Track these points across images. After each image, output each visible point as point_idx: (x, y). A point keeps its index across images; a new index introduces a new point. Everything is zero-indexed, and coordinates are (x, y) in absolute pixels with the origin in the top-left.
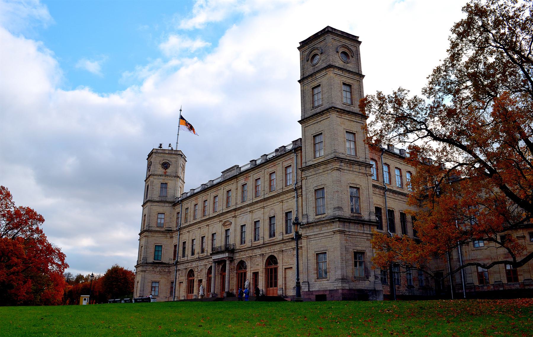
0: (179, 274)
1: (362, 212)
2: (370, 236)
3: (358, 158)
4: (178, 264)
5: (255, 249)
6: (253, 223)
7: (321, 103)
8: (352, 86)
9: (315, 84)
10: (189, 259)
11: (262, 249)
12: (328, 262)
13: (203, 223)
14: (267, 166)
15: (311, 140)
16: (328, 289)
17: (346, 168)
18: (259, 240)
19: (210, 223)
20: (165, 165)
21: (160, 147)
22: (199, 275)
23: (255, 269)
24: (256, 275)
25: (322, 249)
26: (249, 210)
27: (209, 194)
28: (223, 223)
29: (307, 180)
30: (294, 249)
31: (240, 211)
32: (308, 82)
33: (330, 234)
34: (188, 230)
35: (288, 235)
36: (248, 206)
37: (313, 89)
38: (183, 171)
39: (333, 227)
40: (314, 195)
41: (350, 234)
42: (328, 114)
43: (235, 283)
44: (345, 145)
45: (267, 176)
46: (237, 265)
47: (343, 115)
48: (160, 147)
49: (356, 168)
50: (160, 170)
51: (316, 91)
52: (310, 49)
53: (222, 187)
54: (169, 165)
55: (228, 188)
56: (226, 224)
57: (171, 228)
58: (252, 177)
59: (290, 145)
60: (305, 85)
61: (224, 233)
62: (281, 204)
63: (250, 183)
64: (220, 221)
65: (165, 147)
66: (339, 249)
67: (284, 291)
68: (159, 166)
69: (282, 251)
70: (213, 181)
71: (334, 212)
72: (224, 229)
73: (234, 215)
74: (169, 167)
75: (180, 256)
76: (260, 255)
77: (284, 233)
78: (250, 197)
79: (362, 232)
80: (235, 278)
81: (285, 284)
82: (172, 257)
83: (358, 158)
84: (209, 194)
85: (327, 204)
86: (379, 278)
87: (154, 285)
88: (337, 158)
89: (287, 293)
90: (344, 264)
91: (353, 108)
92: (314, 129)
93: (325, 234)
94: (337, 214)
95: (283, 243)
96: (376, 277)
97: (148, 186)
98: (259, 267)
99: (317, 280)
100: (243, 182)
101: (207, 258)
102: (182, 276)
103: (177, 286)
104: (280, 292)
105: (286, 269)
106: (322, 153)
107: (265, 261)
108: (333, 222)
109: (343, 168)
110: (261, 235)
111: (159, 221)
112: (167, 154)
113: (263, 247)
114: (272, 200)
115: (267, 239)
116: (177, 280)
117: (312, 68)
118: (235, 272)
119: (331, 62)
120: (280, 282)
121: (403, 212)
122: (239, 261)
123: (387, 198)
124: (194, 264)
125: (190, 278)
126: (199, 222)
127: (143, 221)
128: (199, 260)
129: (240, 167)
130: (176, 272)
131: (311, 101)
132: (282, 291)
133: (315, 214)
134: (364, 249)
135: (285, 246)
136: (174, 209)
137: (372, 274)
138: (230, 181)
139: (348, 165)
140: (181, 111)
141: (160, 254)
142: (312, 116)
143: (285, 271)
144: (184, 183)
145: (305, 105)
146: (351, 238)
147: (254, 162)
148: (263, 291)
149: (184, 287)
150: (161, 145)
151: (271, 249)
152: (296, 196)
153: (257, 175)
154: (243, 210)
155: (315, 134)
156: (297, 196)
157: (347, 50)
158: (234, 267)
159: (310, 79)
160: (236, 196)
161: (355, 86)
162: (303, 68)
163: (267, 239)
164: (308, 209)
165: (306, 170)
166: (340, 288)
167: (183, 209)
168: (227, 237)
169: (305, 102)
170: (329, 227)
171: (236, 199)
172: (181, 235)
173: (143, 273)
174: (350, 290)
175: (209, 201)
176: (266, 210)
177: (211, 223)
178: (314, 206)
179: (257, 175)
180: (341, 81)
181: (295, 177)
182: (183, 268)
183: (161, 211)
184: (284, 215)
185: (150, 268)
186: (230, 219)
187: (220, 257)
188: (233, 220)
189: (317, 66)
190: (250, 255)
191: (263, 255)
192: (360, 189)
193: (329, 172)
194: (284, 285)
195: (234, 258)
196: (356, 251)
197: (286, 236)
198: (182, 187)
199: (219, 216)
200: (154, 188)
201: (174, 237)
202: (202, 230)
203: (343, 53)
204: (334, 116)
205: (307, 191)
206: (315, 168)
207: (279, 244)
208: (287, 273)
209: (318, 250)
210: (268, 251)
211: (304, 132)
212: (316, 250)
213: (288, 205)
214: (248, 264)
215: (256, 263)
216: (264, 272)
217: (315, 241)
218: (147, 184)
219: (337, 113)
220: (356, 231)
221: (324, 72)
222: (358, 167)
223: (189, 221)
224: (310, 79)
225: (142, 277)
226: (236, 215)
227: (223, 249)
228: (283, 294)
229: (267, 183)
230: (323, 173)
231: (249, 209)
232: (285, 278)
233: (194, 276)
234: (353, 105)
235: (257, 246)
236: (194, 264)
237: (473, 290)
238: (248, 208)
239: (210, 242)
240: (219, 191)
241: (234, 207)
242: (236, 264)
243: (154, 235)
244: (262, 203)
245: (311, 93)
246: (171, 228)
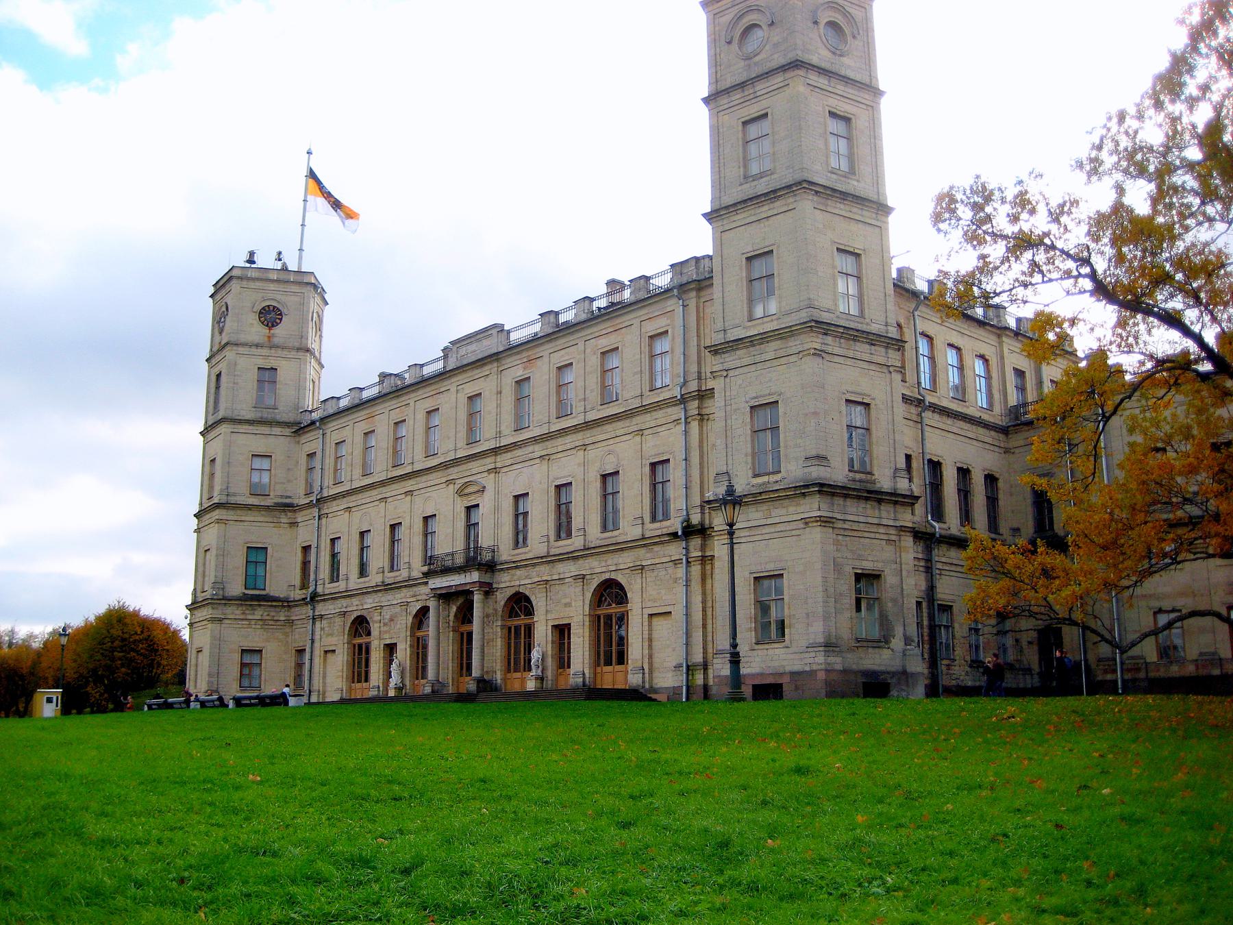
0: (322, 629)
1: (875, 468)
2: (894, 532)
3: (867, 324)
4: (318, 601)
5: (559, 560)
6: (553, 489)
7: (767, 165)
8: (854, 121)
9: (753, 110)
10: (352, 586)
11: (581, 561)
12: (786, 600)
13: (395, 486)
14: (595, 329)
15: (741, 269)
16: (788, 669)
17: (837, 350)
18: (569, 535)
19: (415, 487)
20: (270, 316)
21: (251, 261)
22: (386, 632)
23: (560, 617)
24: (562, 631)
25: (771, 566)
27: (412, 404)
28: (457, 487)
29: (728, 380)
30: (676, 562)
31: (509, 455)
32: (732, 104)
33: (793, 526)
35: (657, 525)
36: (535, 440)
37: (745, 123)
38: (319, 333)
39: (800, 509)
40: (749, 420)
41: (846, 526)
42: (791, 200)
43: (499, 654)
44: (835, 285)
45: (594, 360)
46: (505, 605)
47: (829, 202)
48: (251, 261)
49: (862, 349)
50: (256, 331)
51: (754, 130)
52: (736, 7)
53: (452, 384)
54: (281, 314)
55: (471, 389)
56: (466, 491)
57: (290, 497)
58: (546, 359)
59: (663, 273)
60: (722, 113)
61: (463, 515)
62: (638, 439)
63: (542, 375)
64: (449, 482)
65: (265, 260)
66: (818, 566)
67: (647, 675)
68: (253, 319)
69: (642, 569)
70: (422, 366)
71: (806, 470)
72: (461, 504)
73: (492, 466)
74: (281, 319)
75: (321, 576)
76: (576, 578)
77: (647, 518)
78: (541, 416)
79: (875, 521)
80: (499, 640)
81: (650, 657)
82: (298, 582)
83: (867, 324)
84: (412, 404)
85: (786, 447)
86: (913, 641)
87: (247, 659)
88: (817, 322)
89: (655, 681)
90: (832, 604)
91: (856, 183)
92: (749, 238)
93: (779, 527)
94: (814, 475)
95: (645, 545)
96: (907, 640)
97: (219, 376)
98: (571, 612)
99: (757, 647)
100: (519, 374)
101: (409, 583)
102: (332, 635)
103: (317, 660)
104: (634, 680)
105: (651, 615)
106: (773, 307)
107: (589, 595)
108: (804, 494)
109: (829, 349)
110: (576, 523)
111: (255, 478)
112: (273, 281)
113: (582, 557)
114: (608, 427)
115: (595, 534)
116: (317, 645)
117: (742, 64)
118: (499, 623)
119: (799, 53)
120: (635, 650)
121: (935, 459)
122: (510, 592)
123: (927, 429)
124: (369, 602)
125: (358, 641)
126: (383, 483)
127: (206, 478)
128: (386, 590)
129: (506, 328)
130: (314, 623)
131: (741, 159)
132: (641, 675)
133: (750, 473)
134: (879, 566)
135: (648, 555)
136: (299, 442)
137: (899, 631)
138: (477, 368)
139: (842, 341)
140: (309, 153)
141: (260, 572)
142: (745, 201)
143: (650, 625)
144: (322, 367)
145: (722, 169)
146: (848, 538)
147: (552, 318)
148: (584, 674)
149: (340, 663)
150: (252, 254)
151: (609, 562)
152: (683, 419)
153: (563, 356)
154: (518, 452)
155: (753, 254)
156: (686, 418)
157: (840, 17)
158: (496, 610)
159: (738, 96)
160: (499, 414)
161: (861, 122)
162: (716, 64)
163: (595, 534)
164: (730, 458)
165: (727, 352)
166: (820, 667)
167: (328, 445)
168: (471, 526)
169: (722, 161)
170: (792, 509)
171: (498, 423)
172: (324, 520)
173: (216, 626)
174: (845, 671)
175: (411, 422)
176: (592, 453)
177: (420, 486)
178: (749, 450)
179: (563, 356)
180: (824, 108)
181: (678, 364)
182: (333, 612)
183: (261, 450)
184: (647, 469)
185: (233, 611)
186: (479, 476)
187: (453, 583)
188: (489, 481)
189: (757, 59)
190: (544, 578)
191: (583, 578)
192: (872, 406)
193: (793, 359)
194: (646, 660)
195: (494, 586)
196: (860, 571)
197: (653, 529)
198: (317, 378)
199: (445, 466)
200: (237, 383)
201: (300, 524)
202: (390, 506)
203: (832, 25)
204: (806, 204)
205: (728, 408)
206: (754, 345)
207: (631, 548)
208: (654, 628)
209: (759, 568)
210: (599, 569)
211: (719, 242)
212: (754, 569)
213: (658, 443)
214: (538, 602)
215: (564, 601)
216: (587, 624)
217: (751, 545)
218: (216, 371)
219: (815, 198)
220: (862, 519)
221: (778, 79)
222: (867, 346)
223: (349, 478)
224: (738, 96)
225: (213, 637)
226: (499, 465)
227: (460, 560)
228: (643, 682)
229: (595, 380)
230: (776, 363)
231: (538, 450)
232: (650, 640)
233: (369, 634)
234: (854, 174)
235: (568, 553)
236: (370, 601)
237: (1142, 675)
238: (537, 447)
239: (418, 540)
240: (441, 395)
241: (492, 444)
242: (503, 603)
243: (243, 518)
244: (580, 436)
245: (740, 135)
246: (290, 497)
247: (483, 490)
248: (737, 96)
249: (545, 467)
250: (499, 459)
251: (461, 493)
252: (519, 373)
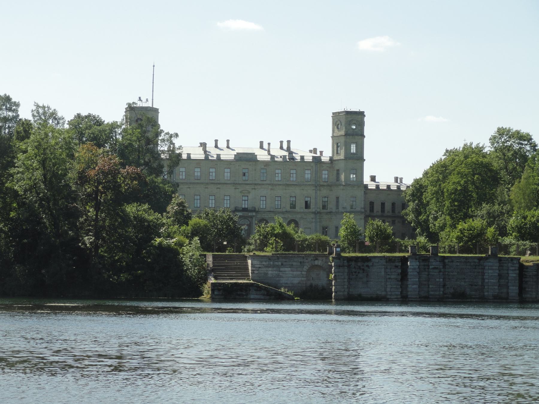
26: (270, 188)
34: (188, 186)
64: (236, 188)
73: (254, 188)
154: (263, 186)
226: (256, 188)
231: (270, 187)
247: (249, 192)
251: (241, 192)
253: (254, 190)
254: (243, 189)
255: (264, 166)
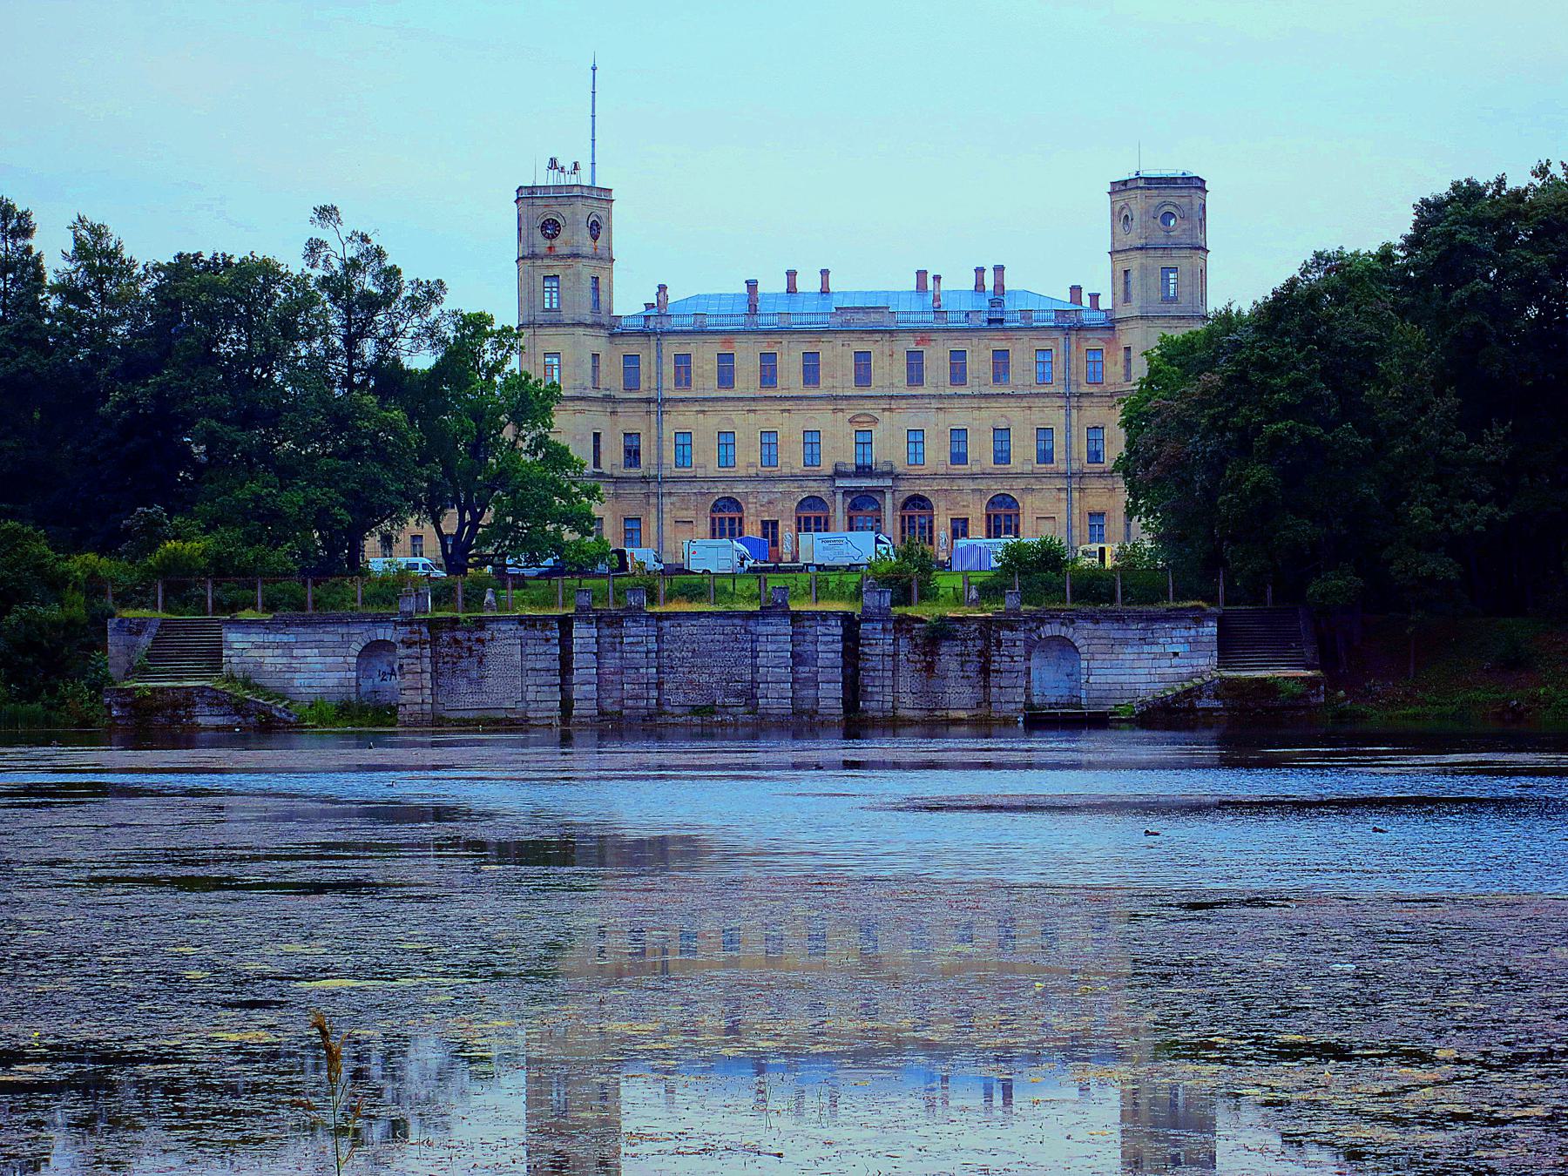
9: (1170, 264)
64: (835, 411)
73: (888, 406)
115: (988, 462)
210: (998, 487)
231: (935, 404)
244: (976, 400)
248: (1160, 252)
249: (941, 415)
250: (893, 402)
252: (913, 347)
253: (887, 413)
254: (859, 412)
255: (917, 344)
